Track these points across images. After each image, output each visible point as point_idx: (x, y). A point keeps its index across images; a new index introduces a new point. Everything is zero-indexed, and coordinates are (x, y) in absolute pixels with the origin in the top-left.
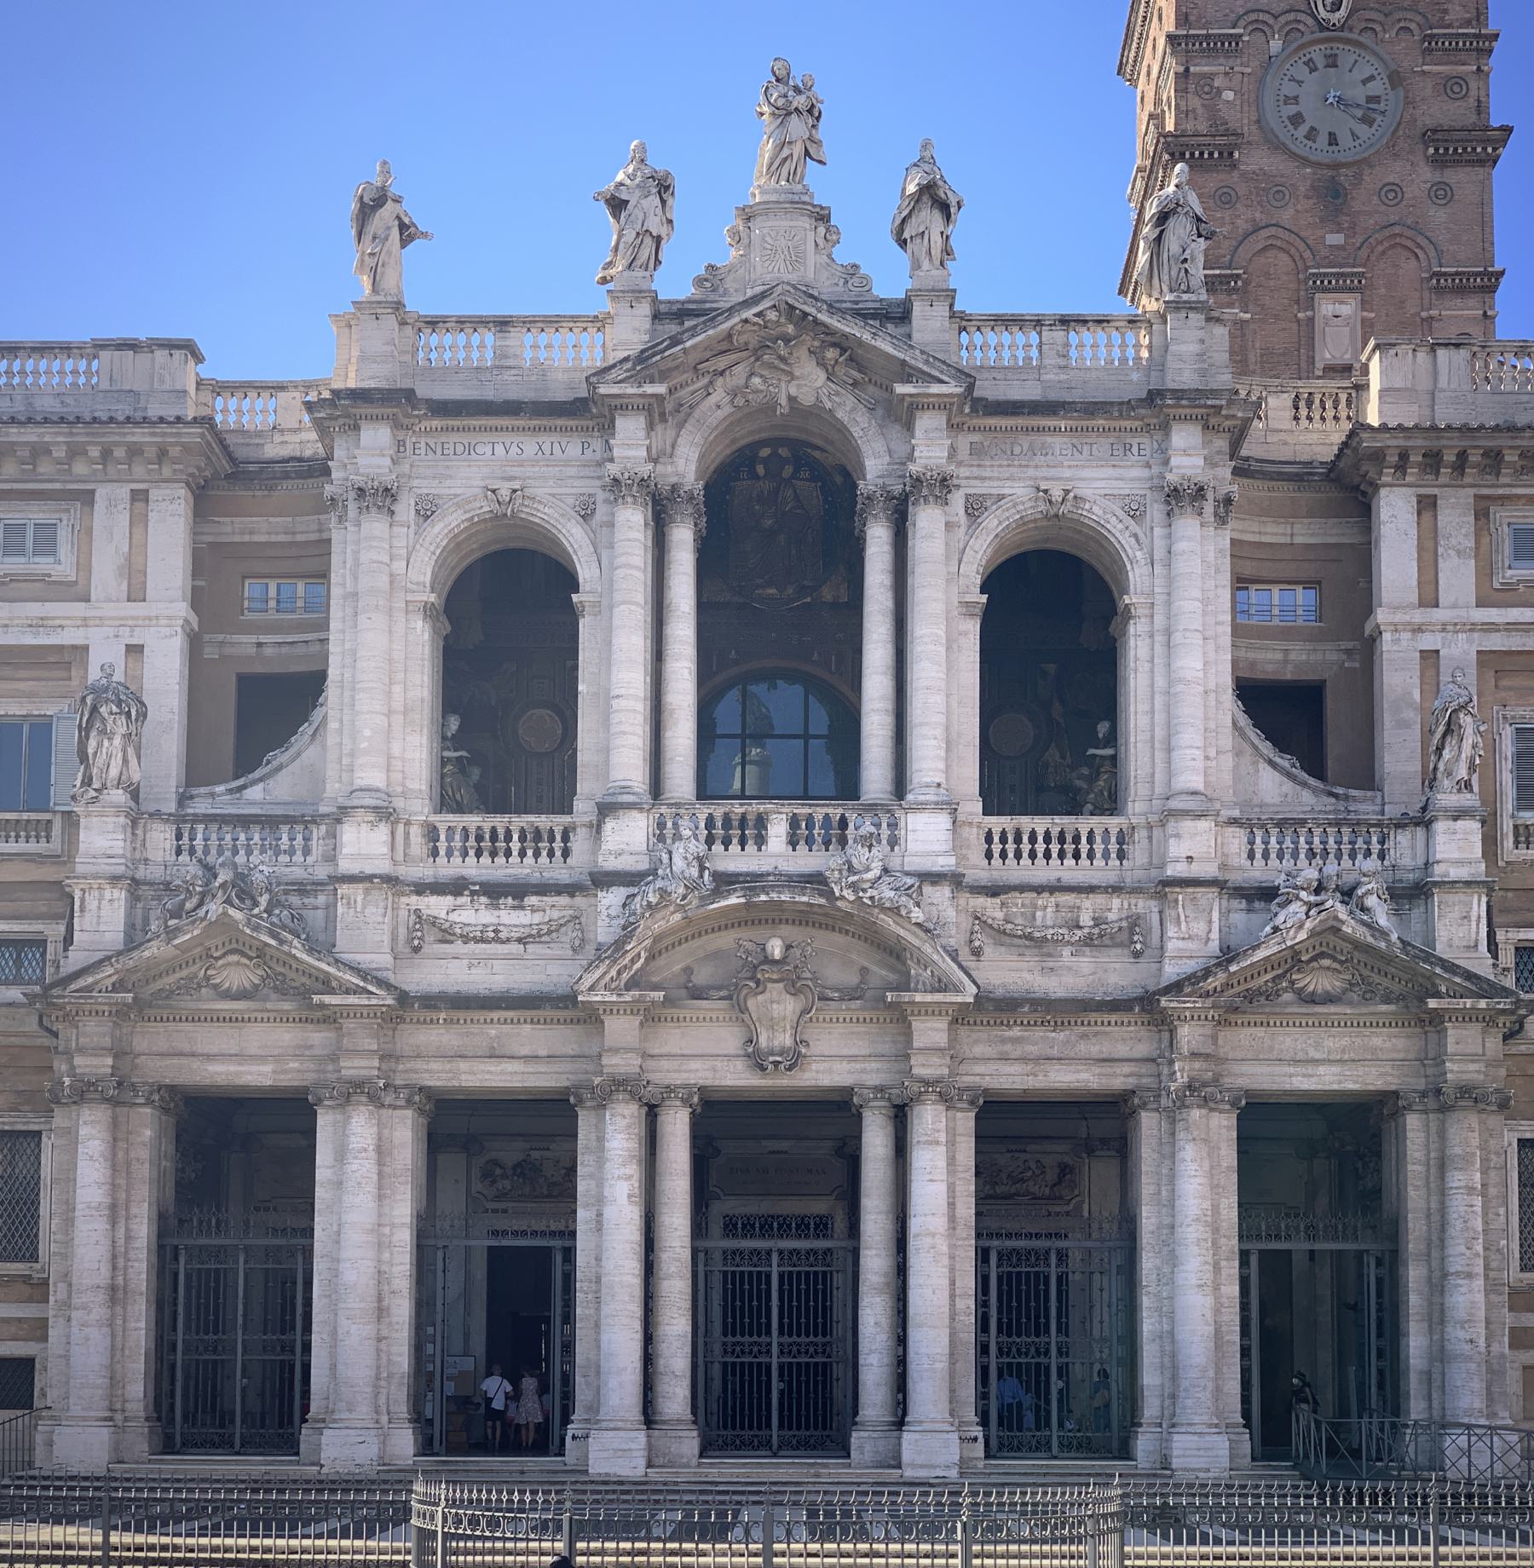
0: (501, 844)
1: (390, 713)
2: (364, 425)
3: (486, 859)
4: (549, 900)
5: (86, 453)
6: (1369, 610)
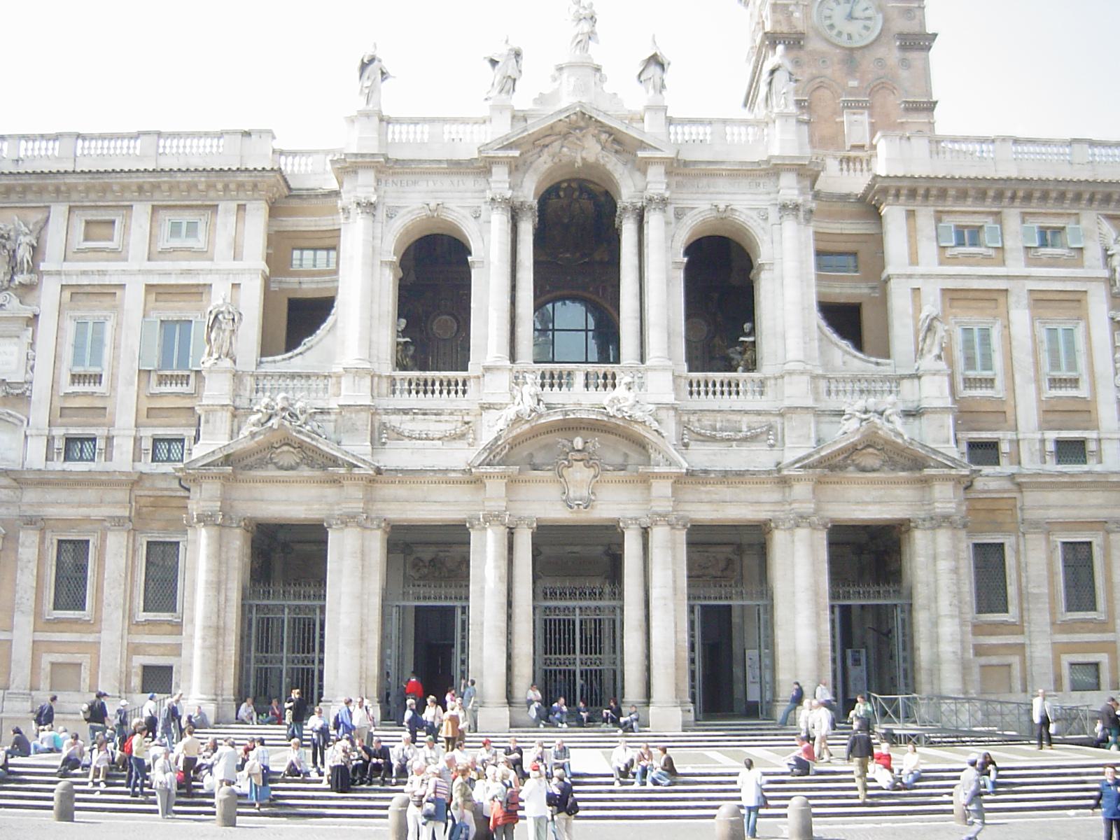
0: (429, 388)
1: (371, 317)
2: (360, 171)
3: (421, 394)
4: (456, 418)
5: (215, 186)
6: (883, 268)
